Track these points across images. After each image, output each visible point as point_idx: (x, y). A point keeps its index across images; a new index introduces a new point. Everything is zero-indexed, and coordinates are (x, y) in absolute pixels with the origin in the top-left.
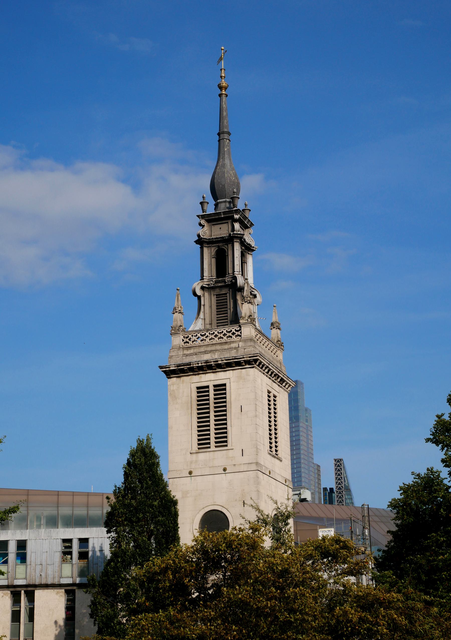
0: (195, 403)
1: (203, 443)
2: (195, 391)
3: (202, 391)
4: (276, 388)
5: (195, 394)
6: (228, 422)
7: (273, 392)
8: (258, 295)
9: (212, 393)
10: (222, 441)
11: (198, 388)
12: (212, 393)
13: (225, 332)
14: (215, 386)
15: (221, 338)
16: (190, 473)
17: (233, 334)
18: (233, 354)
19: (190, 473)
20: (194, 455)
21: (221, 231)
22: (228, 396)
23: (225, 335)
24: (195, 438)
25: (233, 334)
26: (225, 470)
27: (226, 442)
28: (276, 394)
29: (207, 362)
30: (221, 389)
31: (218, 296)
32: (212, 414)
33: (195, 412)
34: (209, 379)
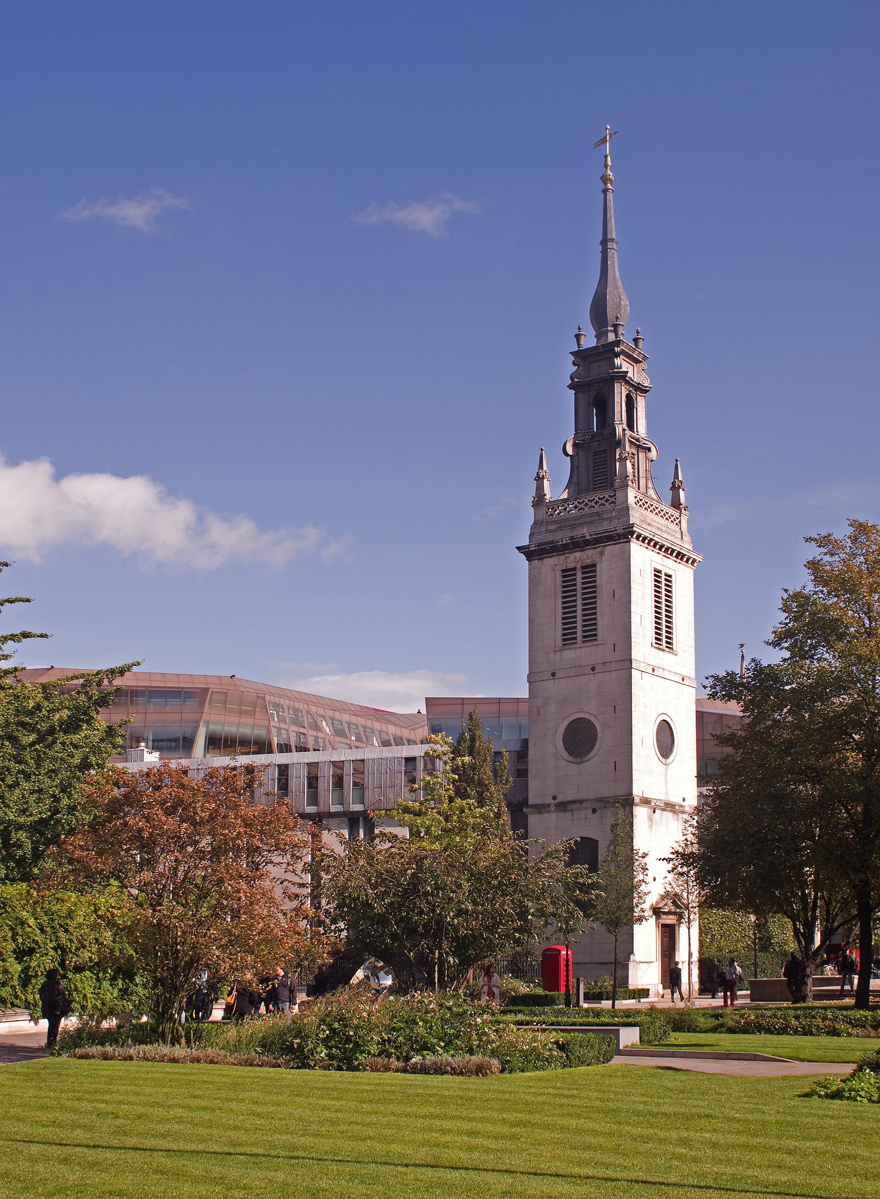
0: (559, 590)
1: (568, 638)
2: (559, 574)
3: (568, 573)
4: (669, 565)
5: (559, 580)
6: (598, 611)
7: (664, 570)
8: (653, 449)
9: (579, 576)
10: (591, 635)
11: (563, 571)
12: (579, 576)
13: (597, 499)
14: (583, 568)
15: (581, 509)
16: (553, 674)
17: (607, 500)
18: (605, 526)
19: (553, 674)
20: (558, 654)
21: (597, 370)
22: (598, 579)
23: (597, 503)
24: (560, 631)
25: (607, 500)
26: (593, 669)
27: (595, 635)
28: (670, 572)
29: (572, 538)
30: (590, 569)
31: (596, 453)
32: (579, 603)
33: (560, 600)
34: (575, 559)
